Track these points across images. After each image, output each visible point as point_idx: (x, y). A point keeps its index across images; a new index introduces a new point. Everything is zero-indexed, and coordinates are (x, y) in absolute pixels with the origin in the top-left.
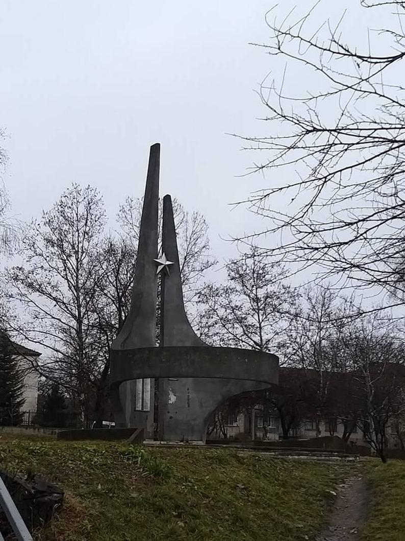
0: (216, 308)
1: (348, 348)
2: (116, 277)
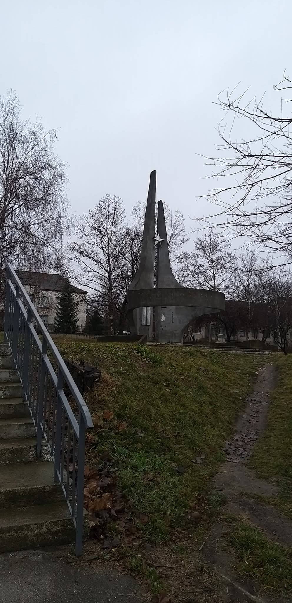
0: (188, 266)
1: (265, 289)
2: (131, 248)
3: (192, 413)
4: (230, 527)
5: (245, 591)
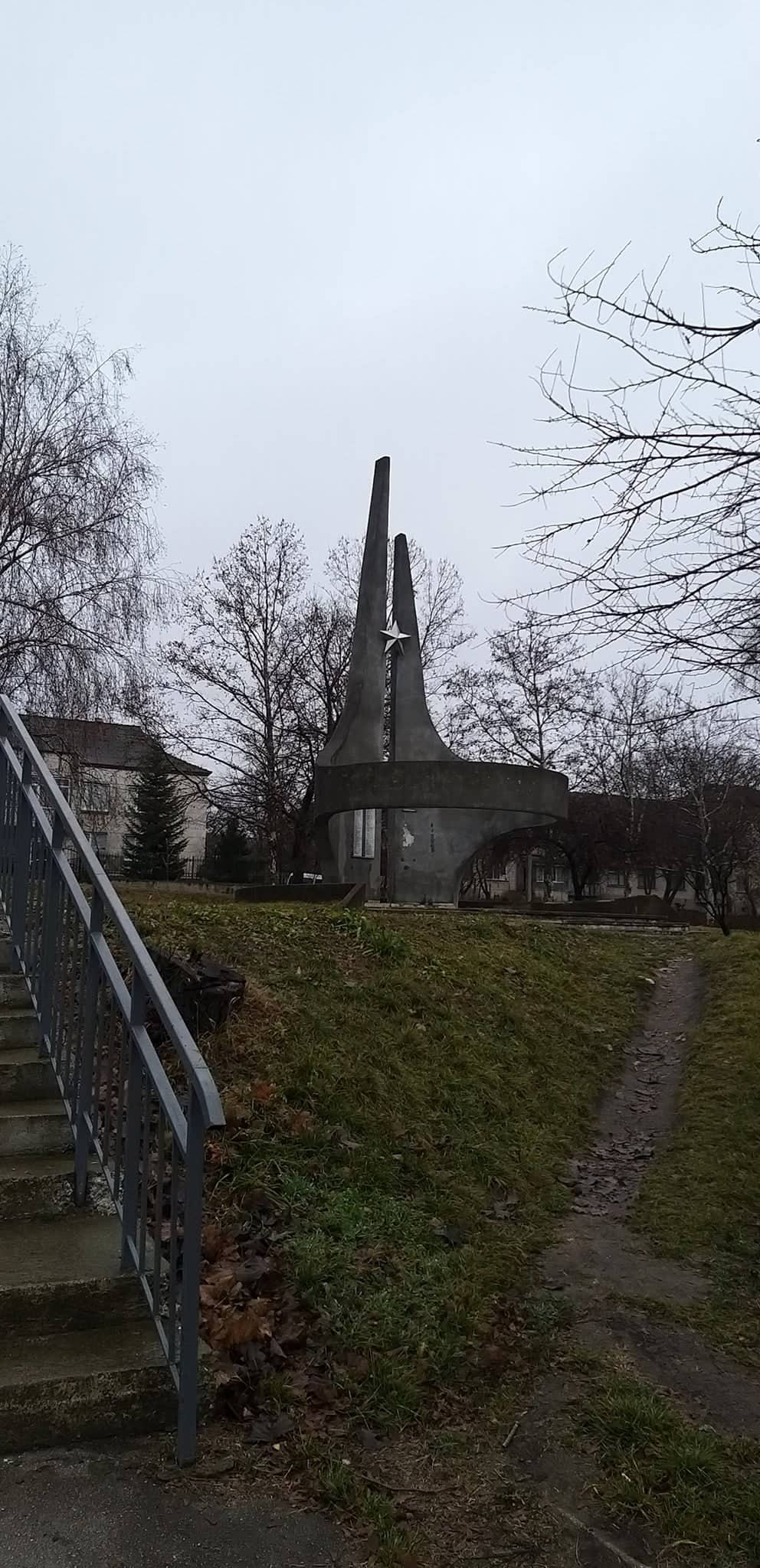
0: (473, 703)
1: (672, 764)
2: (324, 657)
3: (484, 1086)
4: (582, 1385)
5: (622, 1554)
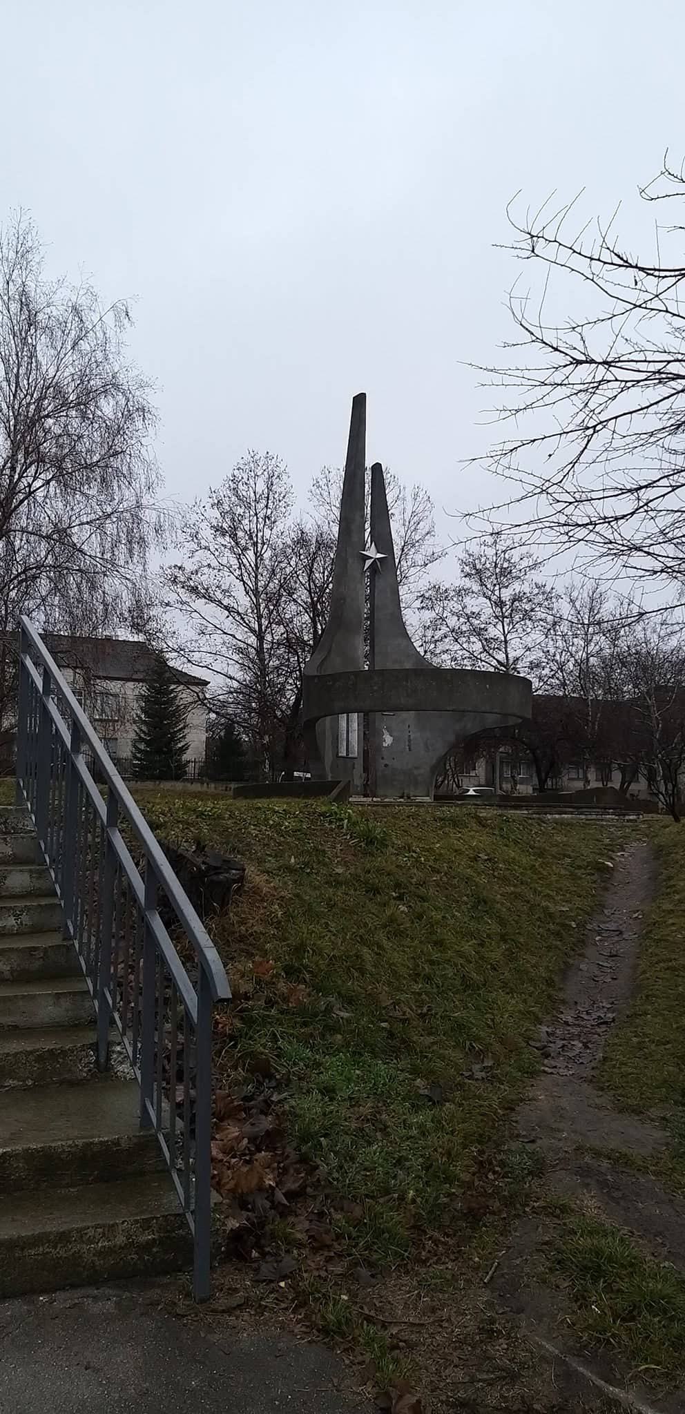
0: (445, 616)
3: (461, 961)
4: (554, 1228)
5: (594, 1378)
